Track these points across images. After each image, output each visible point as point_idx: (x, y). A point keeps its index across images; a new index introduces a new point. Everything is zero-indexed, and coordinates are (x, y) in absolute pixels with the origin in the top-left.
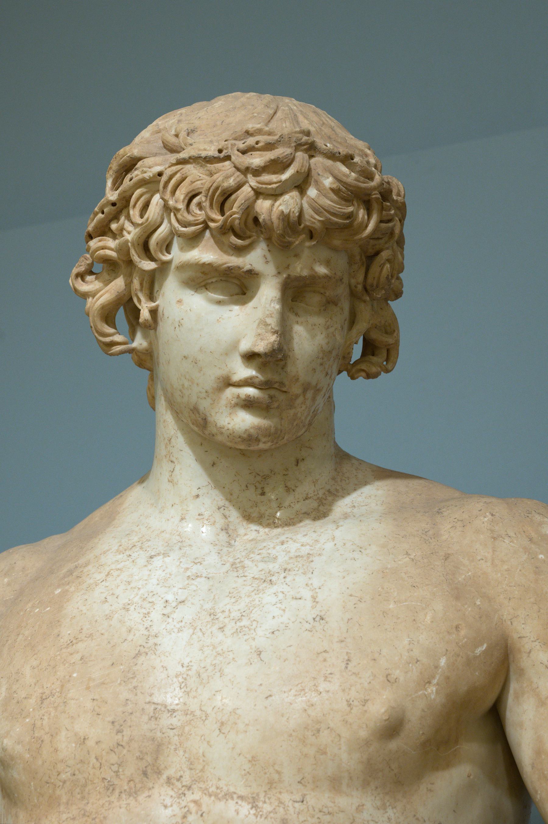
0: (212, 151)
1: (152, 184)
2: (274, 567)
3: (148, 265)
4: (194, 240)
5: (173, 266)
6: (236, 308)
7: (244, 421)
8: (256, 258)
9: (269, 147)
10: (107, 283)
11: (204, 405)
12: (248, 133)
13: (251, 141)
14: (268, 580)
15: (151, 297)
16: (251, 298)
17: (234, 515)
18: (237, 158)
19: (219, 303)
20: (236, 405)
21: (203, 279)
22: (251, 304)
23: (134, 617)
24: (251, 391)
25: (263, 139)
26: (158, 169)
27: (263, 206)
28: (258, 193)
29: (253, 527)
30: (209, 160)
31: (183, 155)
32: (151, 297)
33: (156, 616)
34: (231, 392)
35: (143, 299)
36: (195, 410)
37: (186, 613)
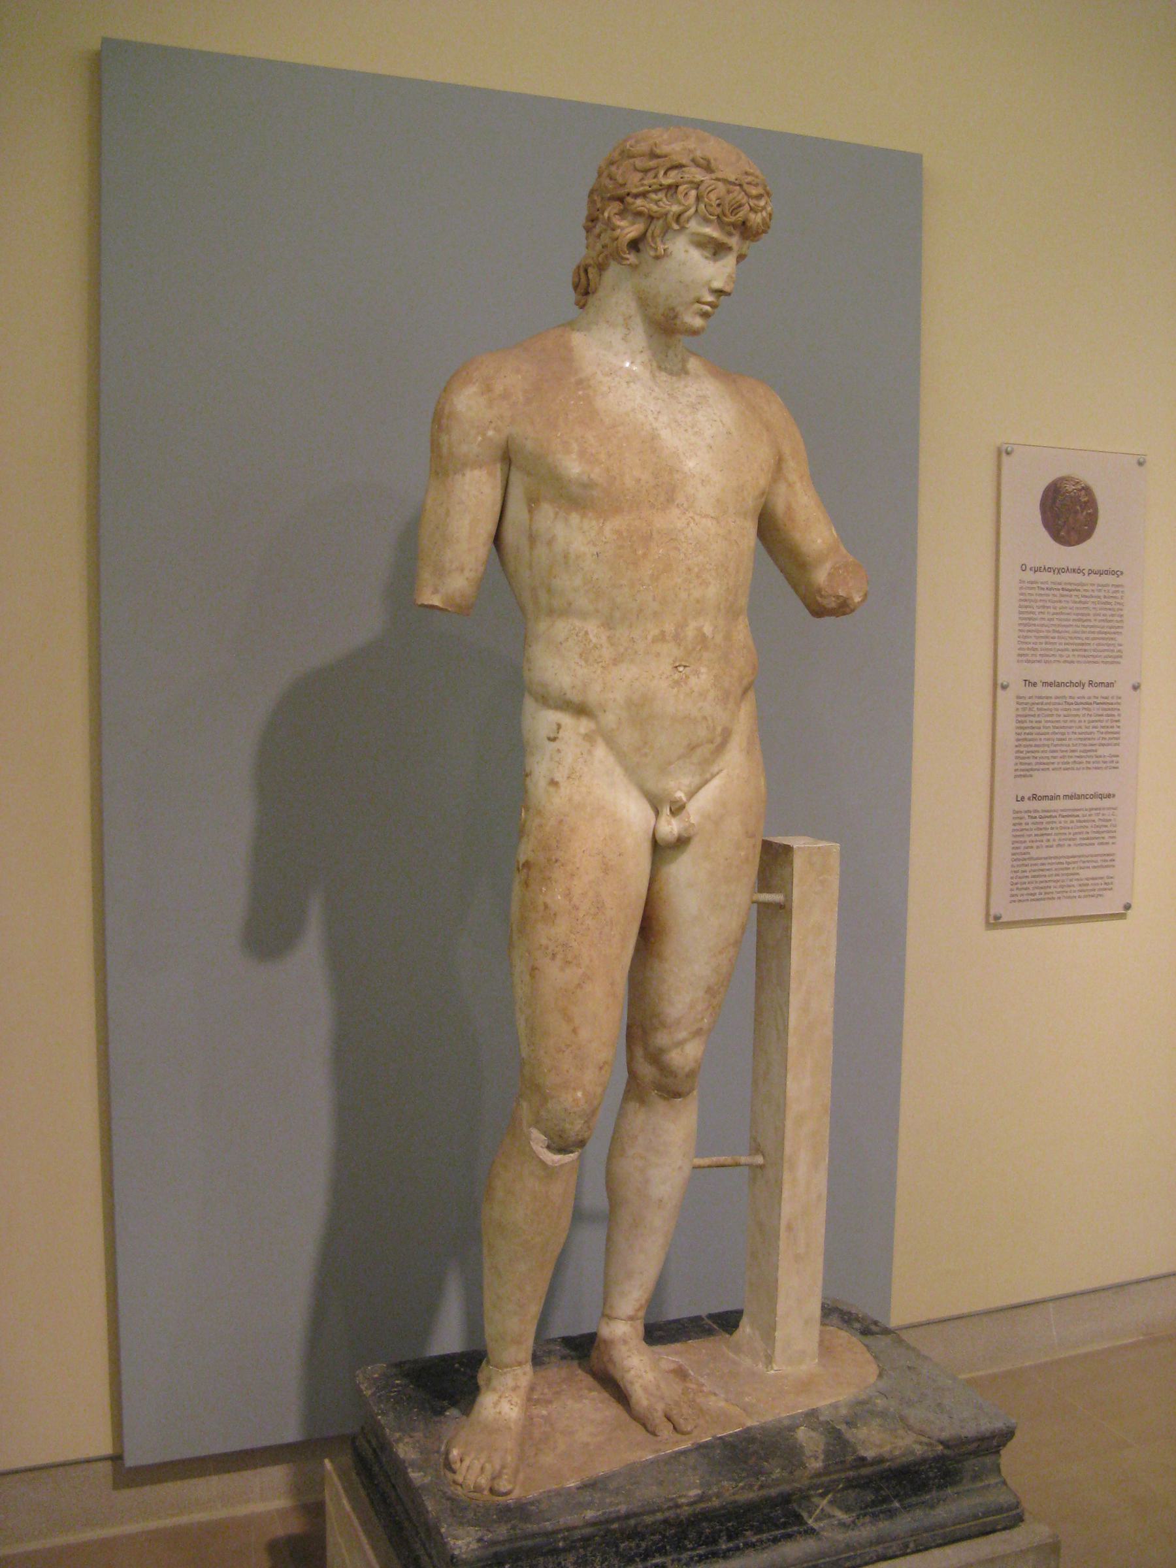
0: (732, 178)
1: (697, 185)
2: (693, 399)
3: (676, 227)
4: (707, 221)
5: (687, 231)
6: (712, 263)
7: (698, 322)
8: (734, 241)
9: (756, 185)
10: (633, 224)
11: (680, 309)
12: (746, 173)
13: (750, 179)
14: (694, 408)
15: (663, 242)
16: (722, 259)
17: (655, 364)
18: (746, 187)
19: (706, 258)
20: (697, 313)
21: (702, 243)
22: (719, 264)
23: (640, 417)
24: (708, 308)
25: (757, 180)
26: (699, 178)
27: (752, 216)
28: (751, 209)
29: (663, 373)
30: (731, 183)
31: (719, 175)
32: (663, 242)
33: (651, 418)
34: (697, 306)
35: (658, 240)
36: (673, 309)
37: (664, 418)
